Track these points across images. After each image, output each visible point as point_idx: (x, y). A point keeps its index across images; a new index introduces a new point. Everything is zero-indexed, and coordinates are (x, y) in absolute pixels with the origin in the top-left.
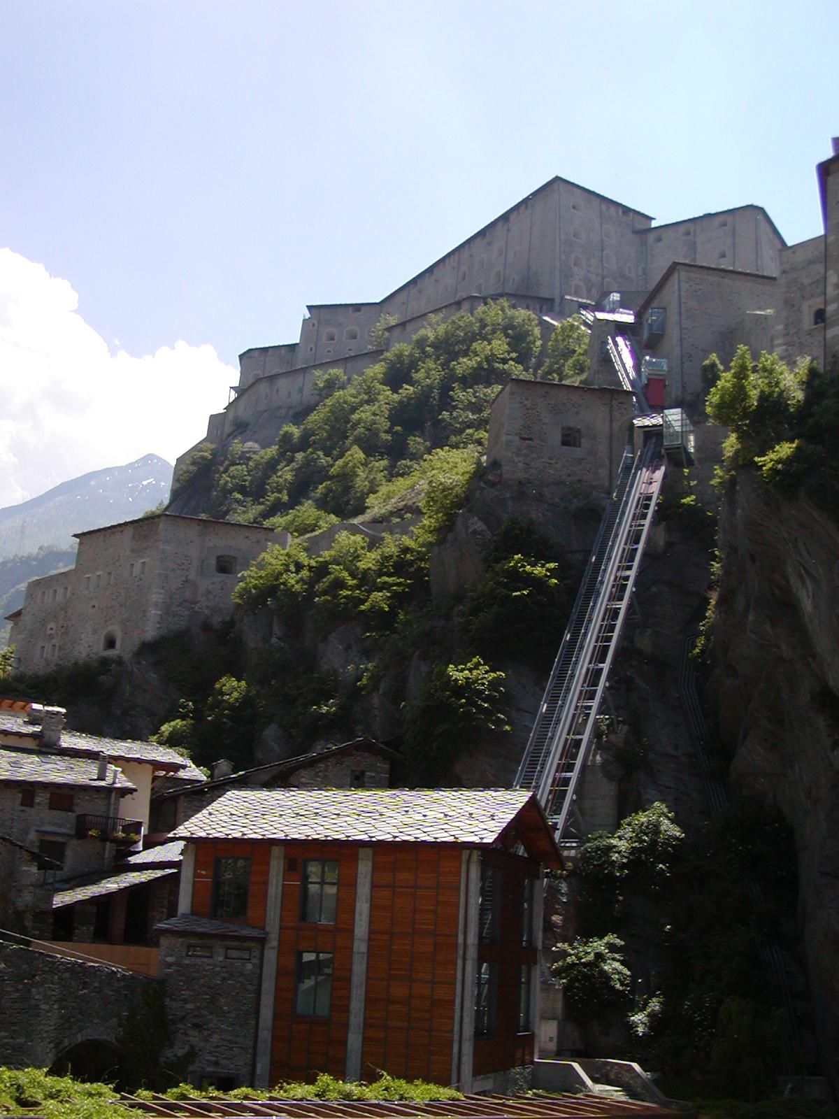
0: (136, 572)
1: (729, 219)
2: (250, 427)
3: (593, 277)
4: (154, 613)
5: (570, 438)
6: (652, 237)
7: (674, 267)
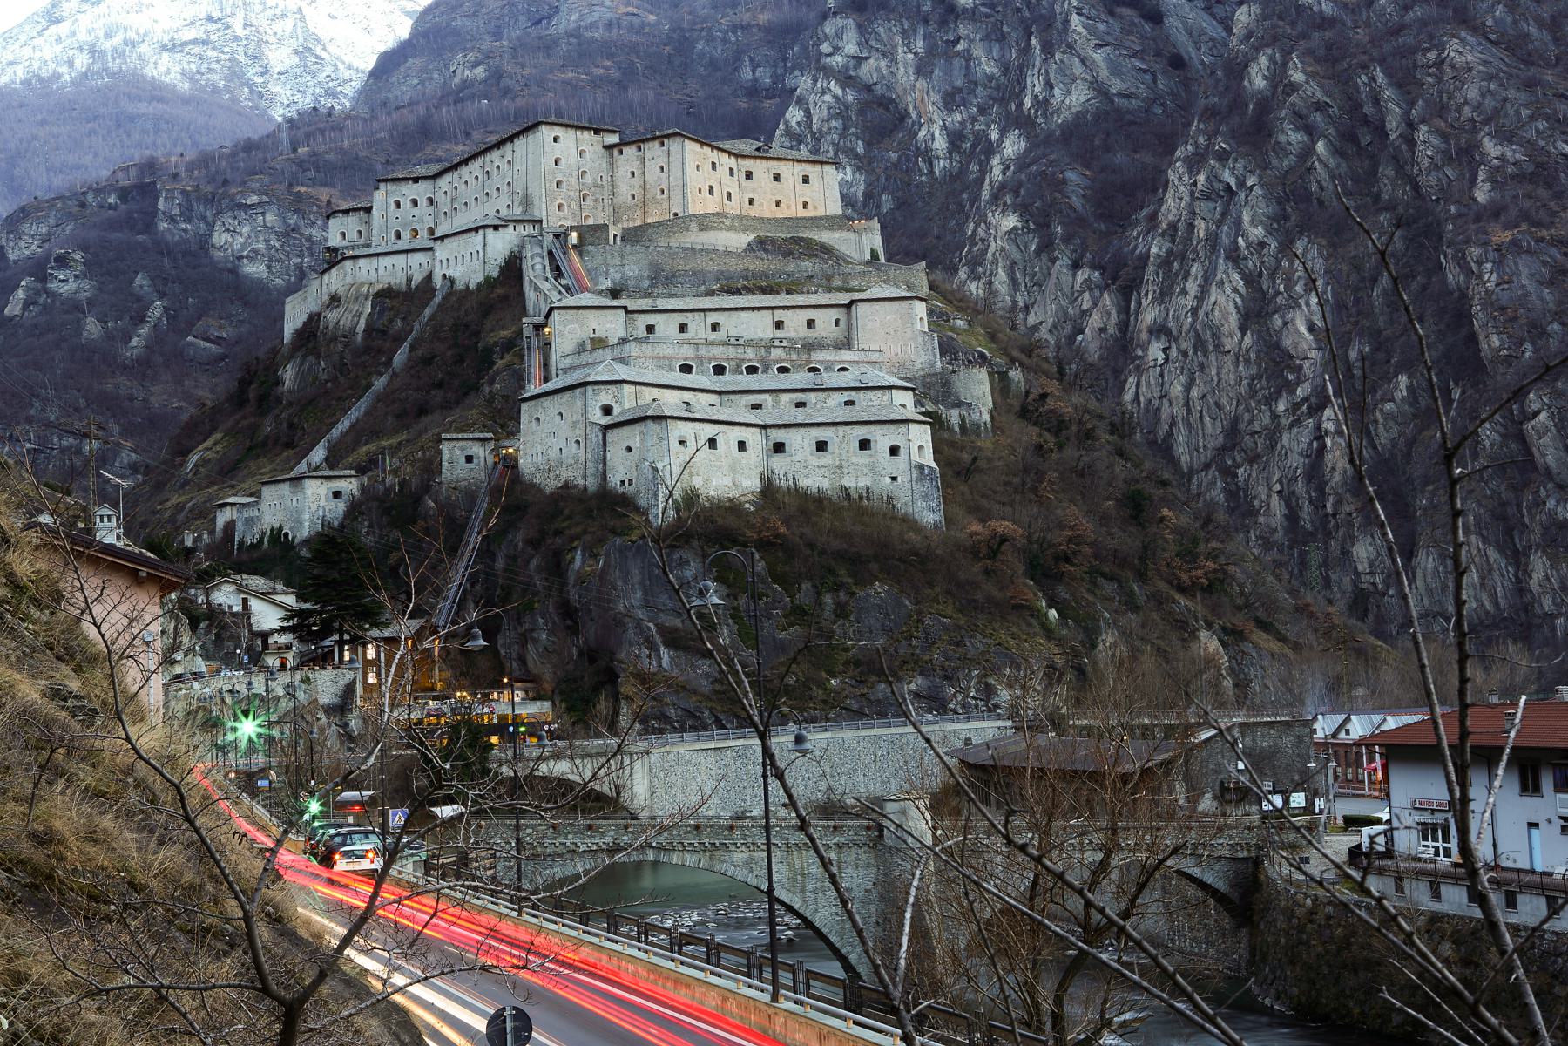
0: (295, 502)
1: (666, 141)
2: (342, 301)
3: (572, 194)
4: (307, 524)
5: (469, 459)
6: (616, 152)
7: (551, 310)
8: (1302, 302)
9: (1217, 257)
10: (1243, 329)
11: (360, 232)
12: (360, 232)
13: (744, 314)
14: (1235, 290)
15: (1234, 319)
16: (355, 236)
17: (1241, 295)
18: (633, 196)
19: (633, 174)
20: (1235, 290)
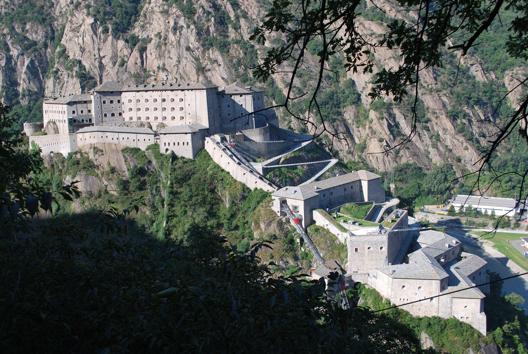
8: (217, 69)
9: (183, 49)
10: (198, 75)
11: (82, 112)
12: (82, 112)
13: (338, 188)
14: (192, 62)
15: (194, 71)
16: (80, 113)
17: (195, 64)
18: (229, 114)
19: (229, 106)
20: (192, 62)
